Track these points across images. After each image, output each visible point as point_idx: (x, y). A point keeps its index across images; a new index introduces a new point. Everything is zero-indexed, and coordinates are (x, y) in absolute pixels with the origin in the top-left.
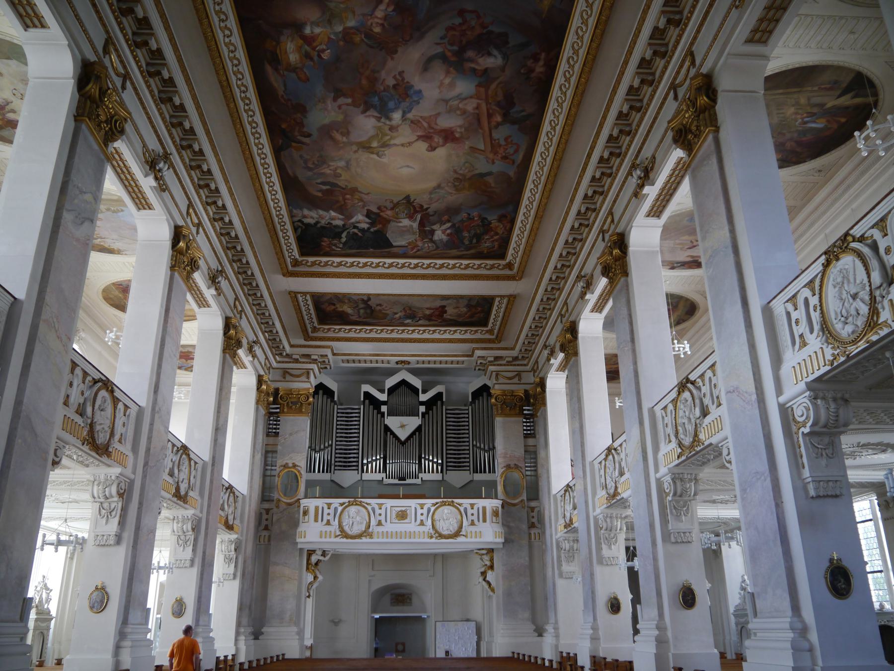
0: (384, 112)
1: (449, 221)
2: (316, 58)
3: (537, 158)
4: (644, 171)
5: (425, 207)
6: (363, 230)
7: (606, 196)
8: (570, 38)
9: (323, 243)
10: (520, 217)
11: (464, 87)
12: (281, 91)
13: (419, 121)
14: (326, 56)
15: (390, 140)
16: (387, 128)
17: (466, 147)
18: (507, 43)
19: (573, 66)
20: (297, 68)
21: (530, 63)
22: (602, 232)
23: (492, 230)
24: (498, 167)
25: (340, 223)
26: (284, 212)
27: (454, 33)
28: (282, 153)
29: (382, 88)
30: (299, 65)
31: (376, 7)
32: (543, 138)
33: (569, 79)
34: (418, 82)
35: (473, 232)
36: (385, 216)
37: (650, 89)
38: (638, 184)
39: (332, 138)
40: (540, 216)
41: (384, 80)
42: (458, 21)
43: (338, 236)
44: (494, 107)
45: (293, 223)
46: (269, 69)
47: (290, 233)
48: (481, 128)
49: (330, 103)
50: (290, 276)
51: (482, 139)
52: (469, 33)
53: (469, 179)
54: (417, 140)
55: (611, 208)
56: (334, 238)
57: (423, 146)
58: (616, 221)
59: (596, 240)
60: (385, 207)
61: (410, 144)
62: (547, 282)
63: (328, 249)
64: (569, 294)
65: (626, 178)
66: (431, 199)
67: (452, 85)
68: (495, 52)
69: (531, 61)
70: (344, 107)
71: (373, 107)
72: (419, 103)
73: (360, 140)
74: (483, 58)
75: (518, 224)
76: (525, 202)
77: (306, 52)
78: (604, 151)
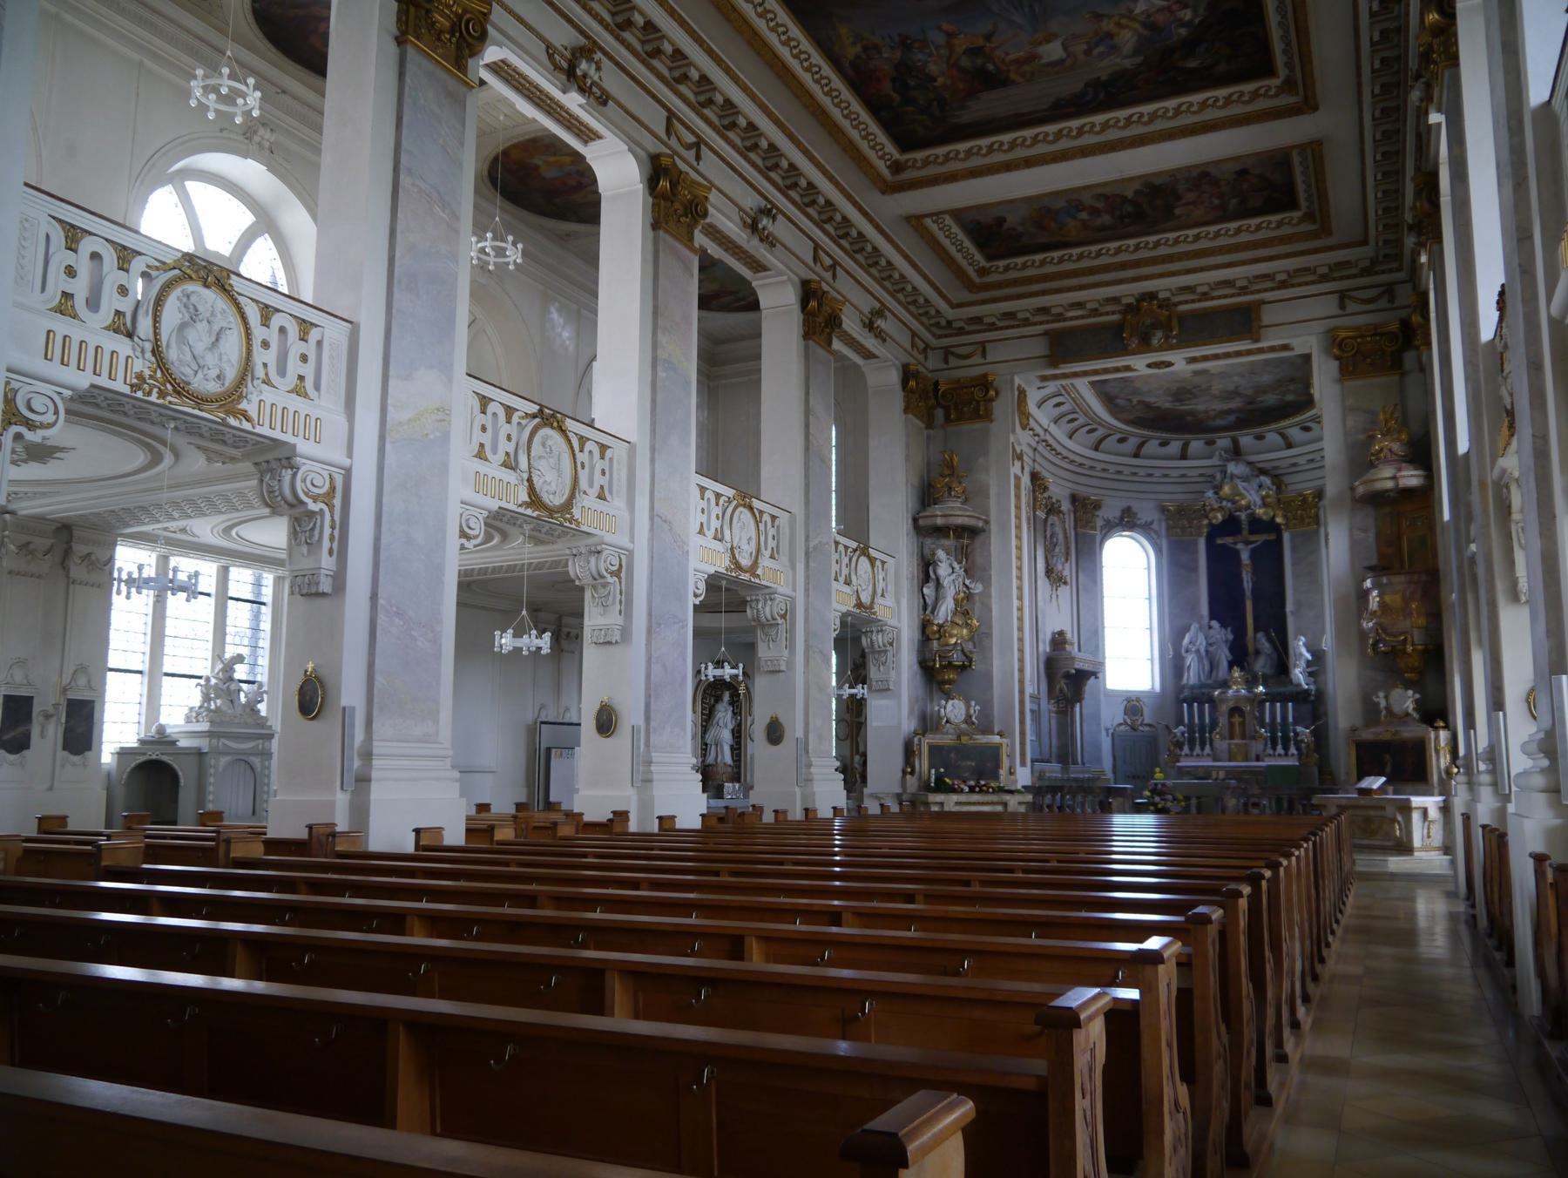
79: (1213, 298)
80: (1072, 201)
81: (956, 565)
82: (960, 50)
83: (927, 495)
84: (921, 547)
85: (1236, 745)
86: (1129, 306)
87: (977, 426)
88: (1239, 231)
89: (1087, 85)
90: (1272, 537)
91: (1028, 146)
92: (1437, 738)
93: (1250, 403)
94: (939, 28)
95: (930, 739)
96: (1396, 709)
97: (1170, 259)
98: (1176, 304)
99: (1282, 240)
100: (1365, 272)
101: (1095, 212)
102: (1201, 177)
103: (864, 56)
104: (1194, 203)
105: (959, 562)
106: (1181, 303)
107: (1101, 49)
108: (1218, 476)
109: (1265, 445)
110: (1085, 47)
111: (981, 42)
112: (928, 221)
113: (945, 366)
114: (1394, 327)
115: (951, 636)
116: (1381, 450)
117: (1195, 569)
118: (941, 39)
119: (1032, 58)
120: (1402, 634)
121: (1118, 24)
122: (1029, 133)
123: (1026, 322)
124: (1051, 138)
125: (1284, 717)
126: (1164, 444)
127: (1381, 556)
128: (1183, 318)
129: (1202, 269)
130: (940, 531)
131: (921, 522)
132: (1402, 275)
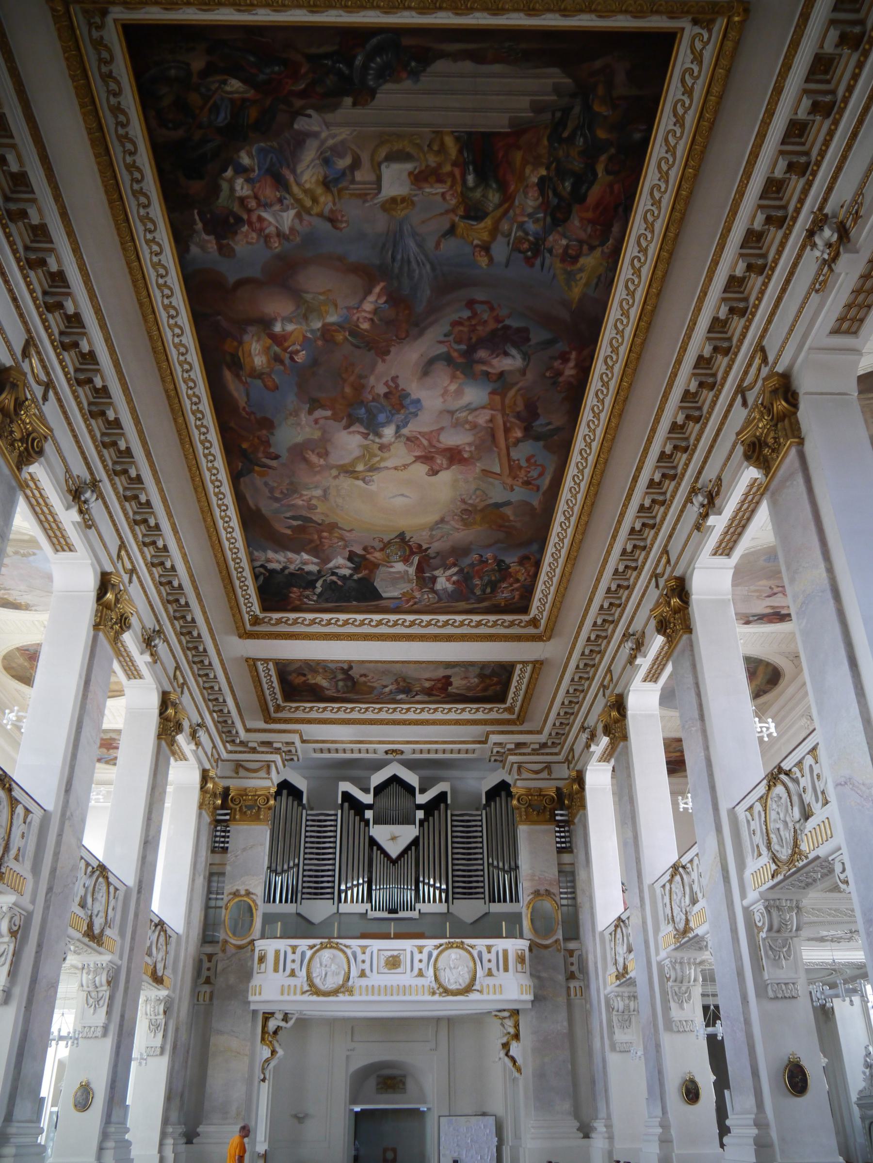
0: (372, 427)
1: (455, 565)
2: (287, 361)
3: (568, 483)
4: (707, 497)
5: (425, 546)
6: (343, 578)
7: (659, 530)
8: (608, 333)
9: (291, 595)
10: (548, 559)
12: (242, 401)
13: (418, 438)
14: (300, 358)
15: (379, 462)
16: (376, 446)
17: (478, 470)
18: (528, 340)
19: (612, 368)
20: (263, 374)
21: (557, 364)
22: (655, 576)
23: (511, 576)
24: (519, 494)
25: (314, 568)
26: (242, 554)
27: (461, 328)
28: (242, 480)
29: (370, 398)
30: (267, 370)
31: (365, 298)
32: (575, 457)
33: (607, 383)
34: (416, 390)
35: (486, 579)
36: (373, 559)
37: (711, 394)
38: (701, 514)
39: (306, 460)
40: (573, 558)
41: (373, 387)
42: (466, 314)
43: (311, 585)
44: (513, 420)
45: (254, 568)
46: (228, 375)
47: (250, 582)
48: (497, 447)
49: (304, 417)
50: (248, 638)
51: (497, 460)
52: (480, 328)
53: (482, 510)
54: (415, 461)
55: (666, 546)
56: (305, 588)
57: (421, 469)
58: (672, 562)
59: (647, 587)
60: (373, 547)
61: (405, 466)
62: (585, 643)
63: (298, 603)
64: (614, 658)
65: (684, 506)
66: (432, 536)
67: (459, 393)
68: (513, 352)
69: (560, 361)
70: (322, 422)
71: (360, 421)
72: (417, 415)
73: (342, 462)
74: (498, 359)
75: (545, 568)
76: (553, 539)
77: (275, 353)
78: (654, 472)
82: (488, 222)
94: (491, 259)
110: (359, 176)
111: (461, 225)
118: (500, 250)
119: (419, 178)
121: (315, 200)
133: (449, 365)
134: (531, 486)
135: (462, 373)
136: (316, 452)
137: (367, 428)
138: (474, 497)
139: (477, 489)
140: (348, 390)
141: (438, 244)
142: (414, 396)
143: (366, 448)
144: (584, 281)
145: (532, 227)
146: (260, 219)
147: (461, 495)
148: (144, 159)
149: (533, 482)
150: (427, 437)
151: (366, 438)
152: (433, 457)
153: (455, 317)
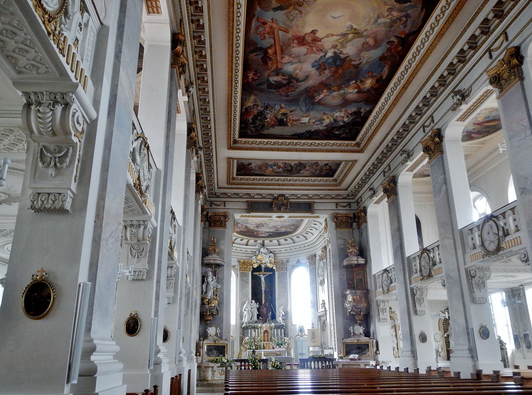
0: (336, 56)
11: (289, 68)
16: (338, 48)
17: (291, 33)
24: (269, 16)
29: (332, 68)
34: (313, 71)
39: (376, 40)
44: (273, 58)
48: (280, 45)
51: (281, 39)
53: (291, 5)
57: (319, 35)
61: (327, 36)
67: (295, 69)
68: (273, 82)
70: (358, 59)
71: (341, 59)
79: (300, 199)
80: (275, 163)
81: (214, 277)
82: (281, 113)
83: (205, 253)
84: (202, 270)
85: (266, 344)
86: (275, 197)
87: (221, 229)
88: (314, 180)
89: (306, 131)
90: (271, 273)
91: (279, 145)
92: (373, 342)
93: (276, 230)
94: (280, 105)
95: (205, 342)
96: (356, 332)
97: (293, 185)
98: (289, 199)
99: (326, 185)
100: (344, 198)
101: (279, 167)
102: (316, 163)
103: (252, 107)
104: (308, 170)
105: (215, 277)
106: (291, 199)
107: (318, 123)
108: (257, 252)
109: (272, 244)
110: (314, 121)
112: (231, 160)
113: (210, 207)
114: (352, 215)
115: (213, 303)
116: (352, 251)
117: (248, 282)
120: (359, 309)
122: (281, 141)
123: (241, 197)
124: (287, 144)
125: (281, 334)
126: (241, 240)
127: (348, 284)
128: (291, 203)
129: (300, 190)
130: (209, 265)
131: (205, 261)
132: (354, 201)
133: (298, 79)
134: (262, 21)
135: (293, 76)
136: (368, 45)
137: (339, 56)
138: (294, 15)
139: (292, 21)
140: (340, 71)
141: (296, 109)
142: (314, 68)
143: (344, 47)
144: (251, 100)
145: (268, 112)
146: (345, 114)
147: (301, 17)
148: (367, 125)
149: (261, 24)
150: (313, 51)
151: (341, 51)
152: (312, 41)
153: (293, 93)
